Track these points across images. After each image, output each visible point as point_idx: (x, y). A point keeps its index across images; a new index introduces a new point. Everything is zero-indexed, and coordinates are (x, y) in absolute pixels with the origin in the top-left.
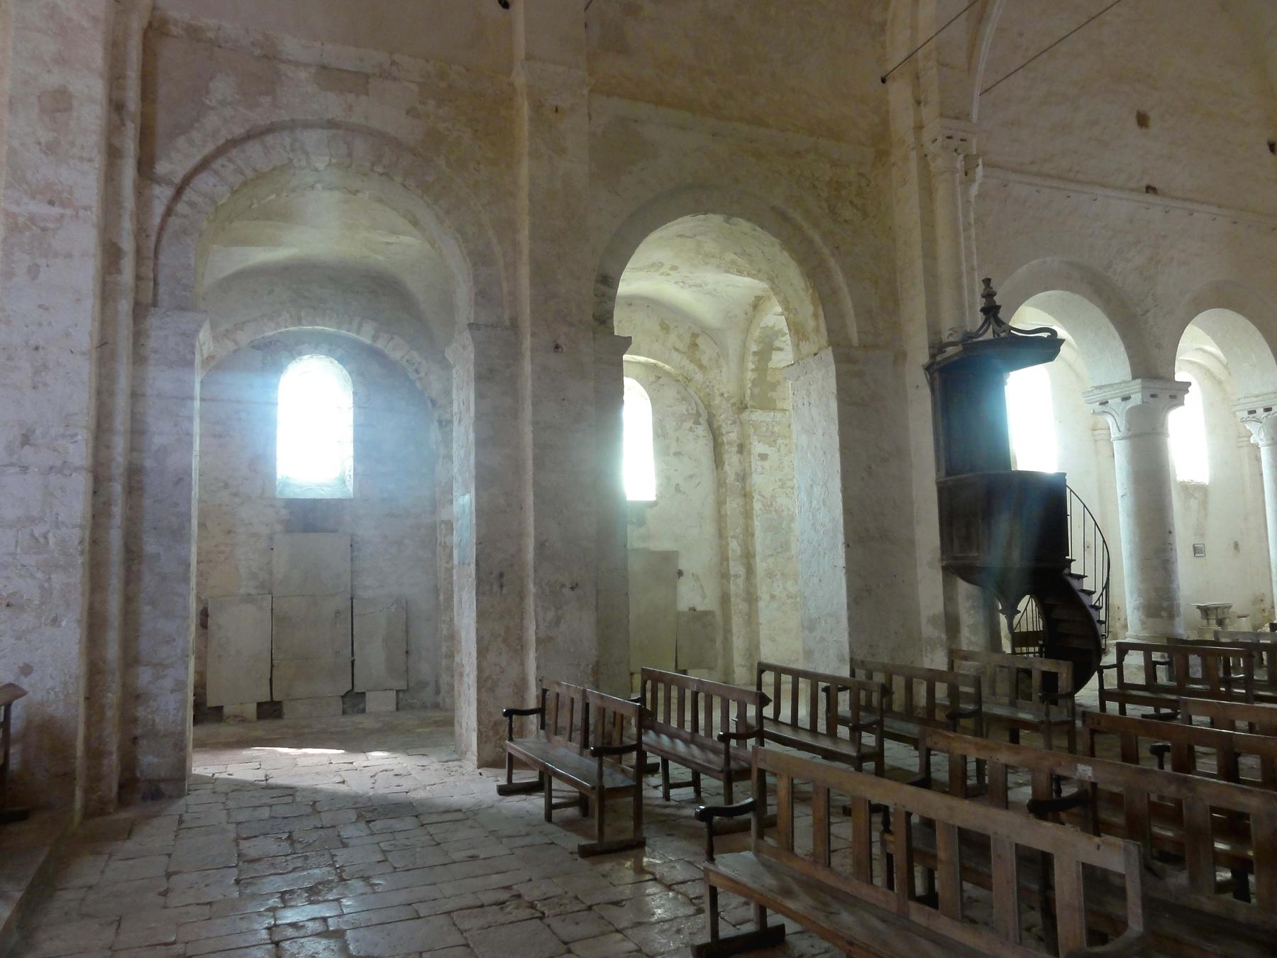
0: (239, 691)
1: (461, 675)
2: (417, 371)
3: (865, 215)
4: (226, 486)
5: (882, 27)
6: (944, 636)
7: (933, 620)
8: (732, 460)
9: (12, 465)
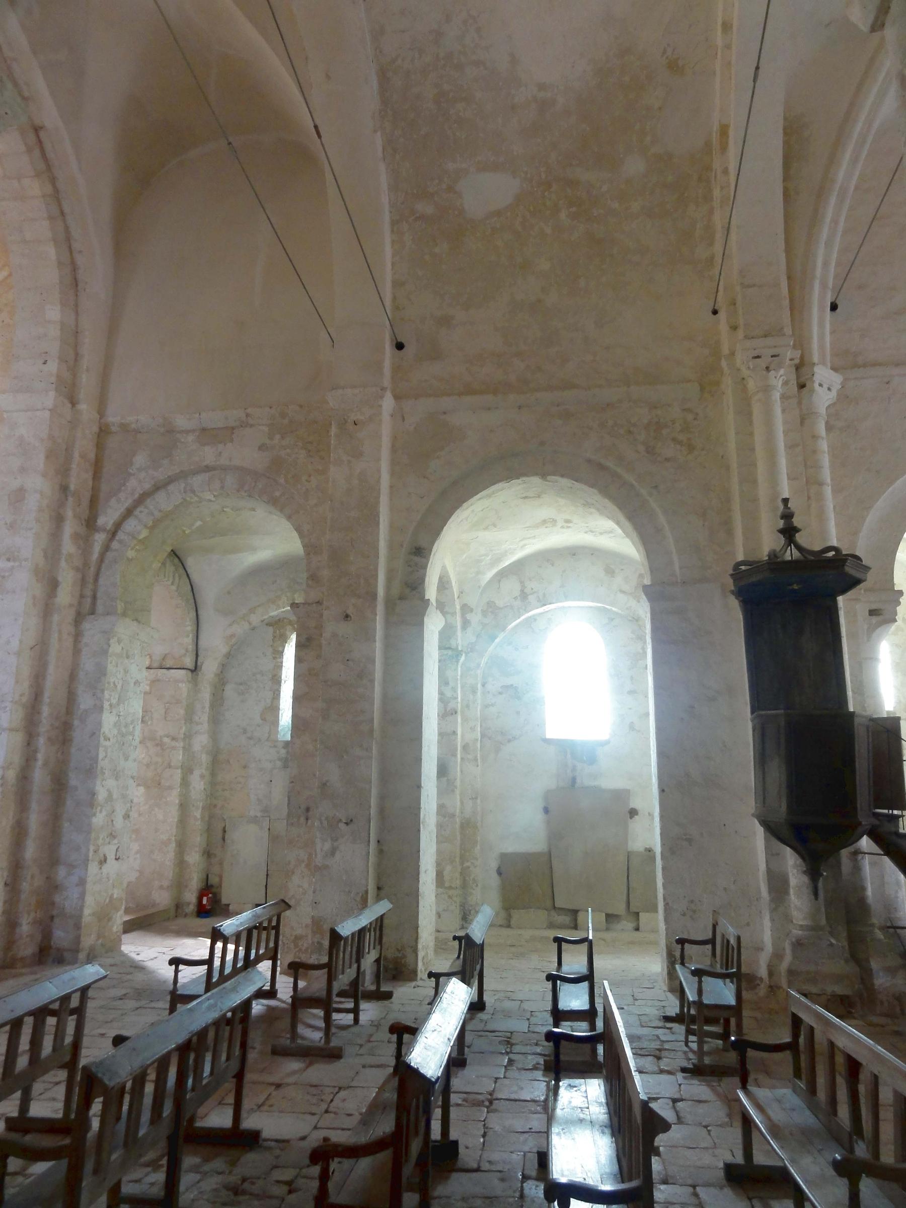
3: (691, 448)
4: (245, 731)
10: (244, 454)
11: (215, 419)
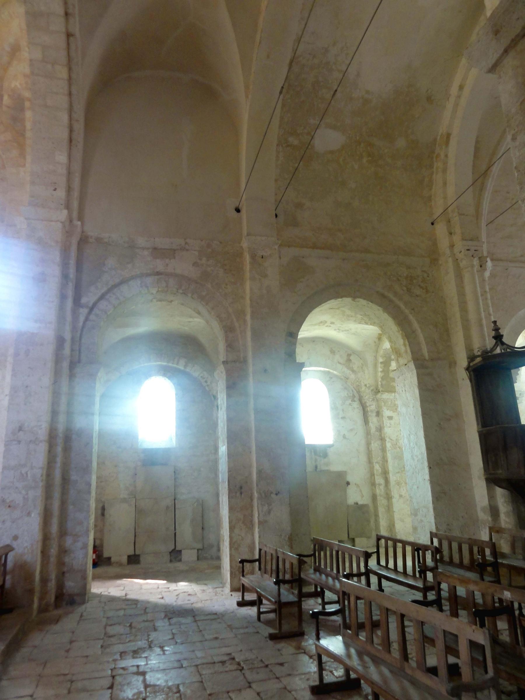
0: (118, 548)
1: (223, 541)
2: (206, 382)
3: (427, 292)
5: (430, 199)
6: (490, 519)
7: (483, 509)
8: (373, 420)
9: (14, 440)
10: (183, 266)
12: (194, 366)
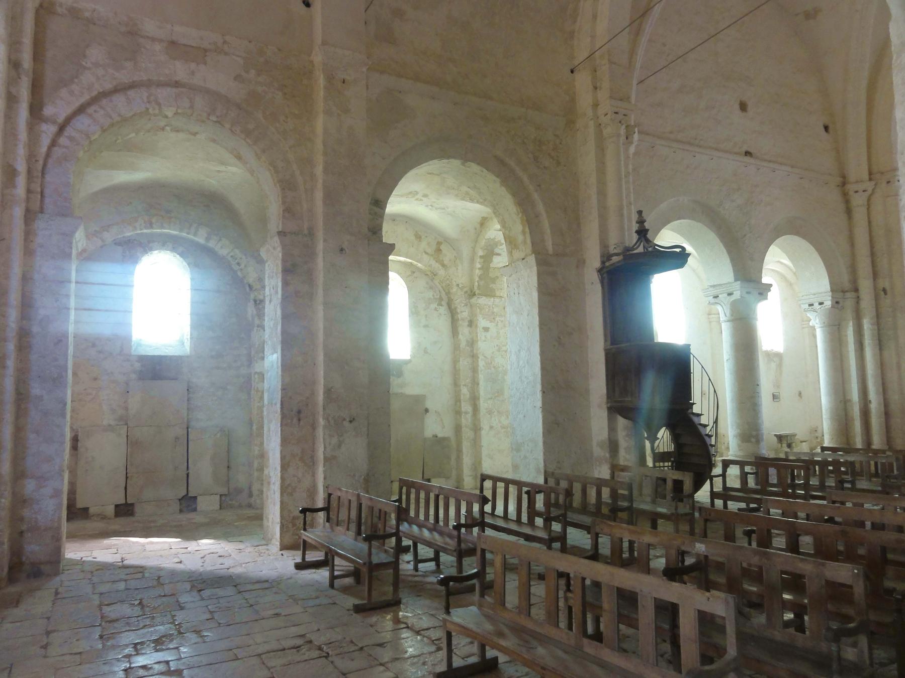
0: (103, 495)
1: (269, 483)
2: (238, 264)
4: (94, 345)
5: (571, 35)
6: (608, 455)
8: (464, 332)
10: (216, 77)
11: (188, 35)
12: (220, 240)
